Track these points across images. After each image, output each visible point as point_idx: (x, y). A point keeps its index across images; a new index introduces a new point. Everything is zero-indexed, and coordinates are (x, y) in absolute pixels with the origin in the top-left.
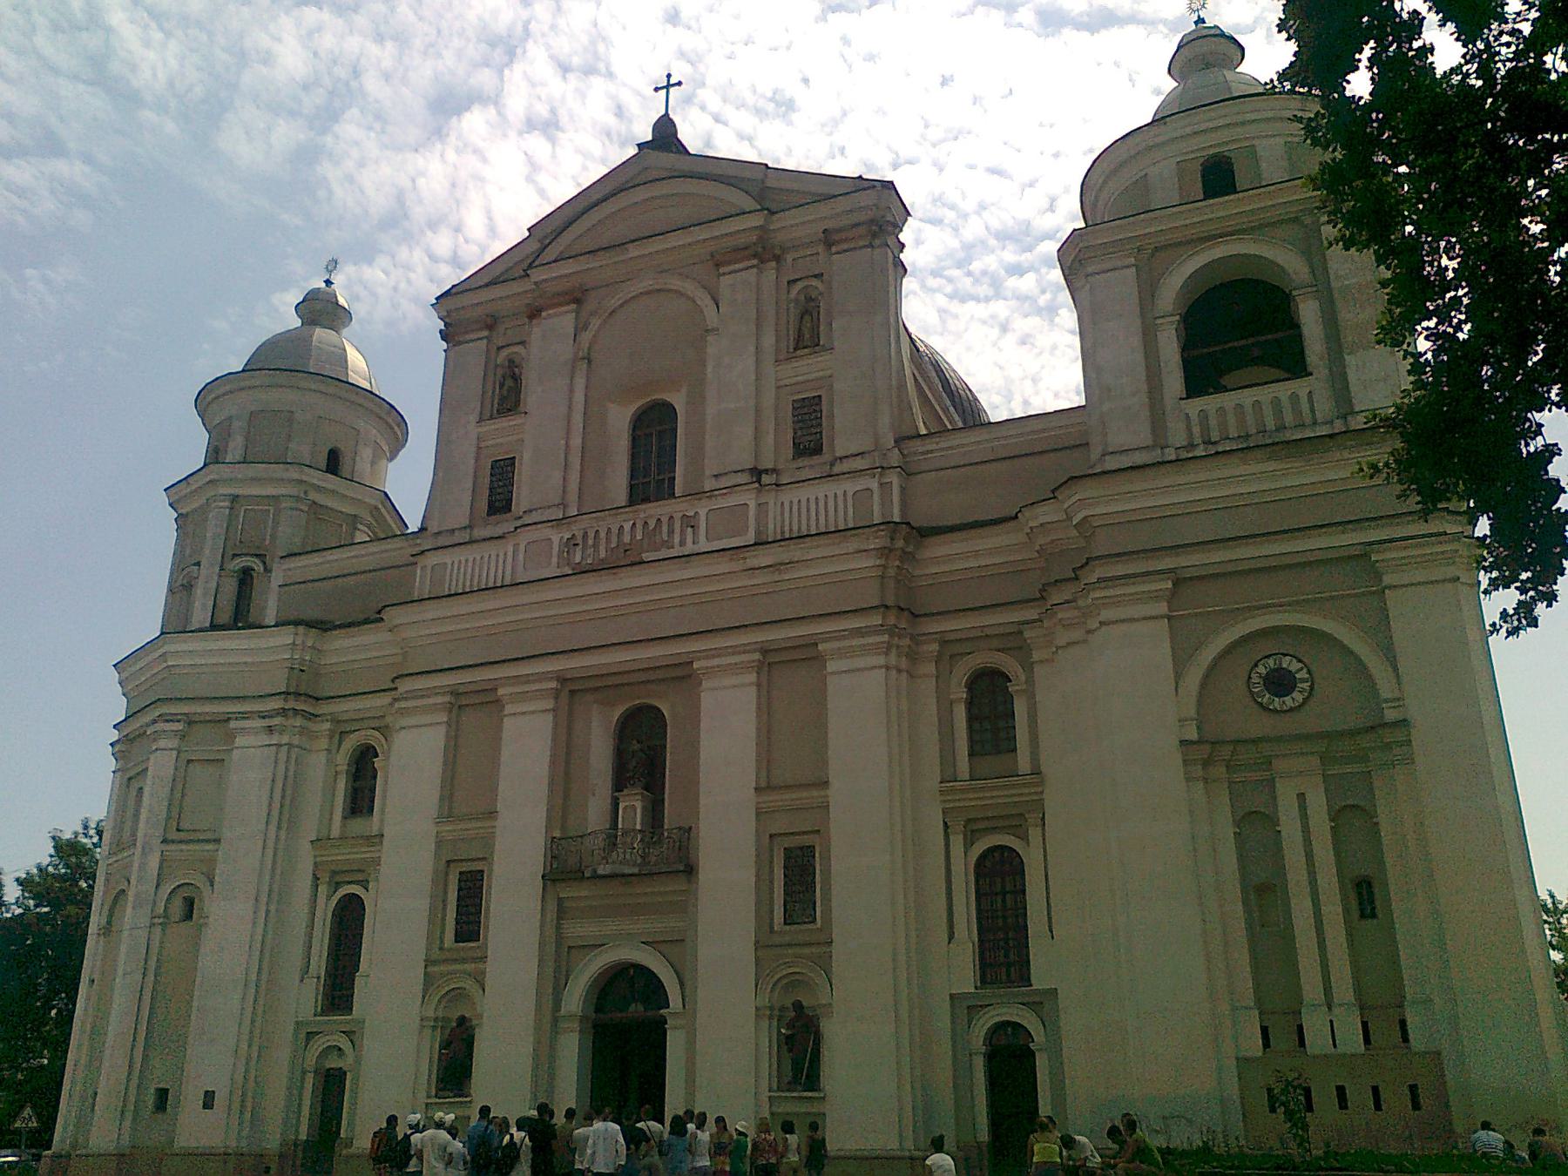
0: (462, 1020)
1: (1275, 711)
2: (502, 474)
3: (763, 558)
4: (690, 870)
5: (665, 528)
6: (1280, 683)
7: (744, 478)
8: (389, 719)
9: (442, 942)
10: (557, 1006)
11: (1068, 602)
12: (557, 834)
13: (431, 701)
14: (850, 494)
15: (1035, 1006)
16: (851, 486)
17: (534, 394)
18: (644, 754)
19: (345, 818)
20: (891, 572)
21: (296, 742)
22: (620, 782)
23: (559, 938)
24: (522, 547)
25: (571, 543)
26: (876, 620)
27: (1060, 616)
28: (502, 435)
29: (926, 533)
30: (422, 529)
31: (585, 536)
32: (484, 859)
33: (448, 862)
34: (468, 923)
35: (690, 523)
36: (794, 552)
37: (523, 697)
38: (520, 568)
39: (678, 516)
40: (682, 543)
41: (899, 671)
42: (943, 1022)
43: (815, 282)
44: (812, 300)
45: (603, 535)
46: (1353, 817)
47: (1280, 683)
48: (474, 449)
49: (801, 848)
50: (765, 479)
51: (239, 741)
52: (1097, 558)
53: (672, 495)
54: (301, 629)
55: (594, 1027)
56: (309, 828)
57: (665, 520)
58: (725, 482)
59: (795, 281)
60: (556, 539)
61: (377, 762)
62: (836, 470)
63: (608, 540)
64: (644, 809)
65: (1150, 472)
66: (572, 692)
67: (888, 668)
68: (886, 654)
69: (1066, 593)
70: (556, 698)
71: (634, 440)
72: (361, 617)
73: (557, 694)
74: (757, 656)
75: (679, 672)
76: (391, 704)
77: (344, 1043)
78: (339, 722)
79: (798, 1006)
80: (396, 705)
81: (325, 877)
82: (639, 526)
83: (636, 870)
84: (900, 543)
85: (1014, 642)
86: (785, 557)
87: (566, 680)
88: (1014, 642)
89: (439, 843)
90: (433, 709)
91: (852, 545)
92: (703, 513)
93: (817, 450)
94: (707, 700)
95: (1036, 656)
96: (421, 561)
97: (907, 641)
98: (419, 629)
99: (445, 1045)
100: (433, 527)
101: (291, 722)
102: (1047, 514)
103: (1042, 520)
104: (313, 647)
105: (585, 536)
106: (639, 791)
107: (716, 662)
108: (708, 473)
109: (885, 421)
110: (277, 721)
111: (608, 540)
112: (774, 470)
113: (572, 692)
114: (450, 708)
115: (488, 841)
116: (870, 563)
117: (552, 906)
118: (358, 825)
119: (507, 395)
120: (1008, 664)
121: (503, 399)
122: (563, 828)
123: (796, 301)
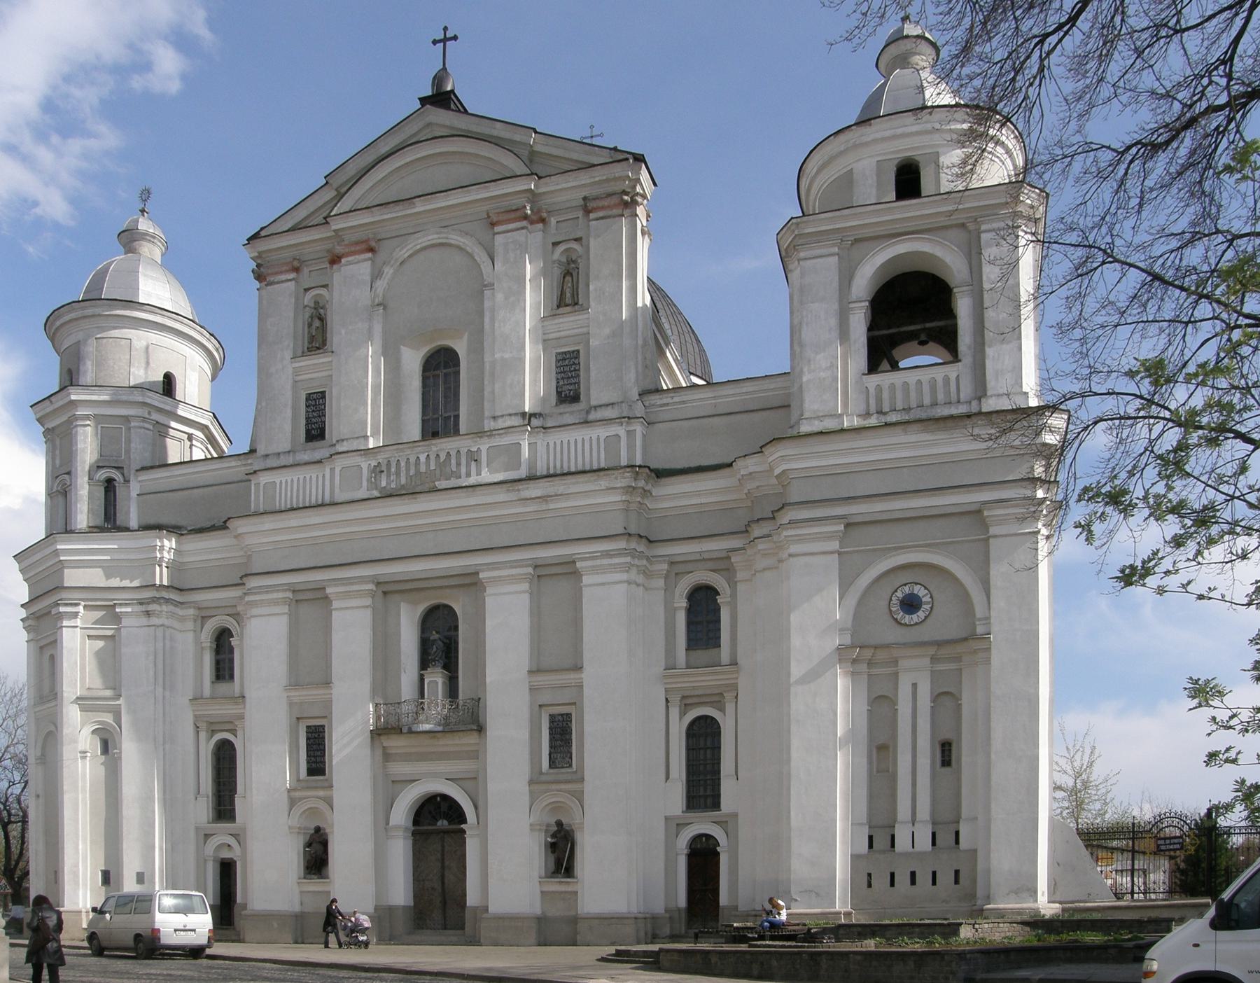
1: (906, 625)
2: (316, 404)
3: (535, 490)
5: (453, 461)
6: (911, 604)
7: (517, 421)
11: (769, 536)
13: (275, 595)
14: (602, 440)
16: (603, 432)
17: (339, 334)
18: (442, 643)
20: (634, 506)
21: (166, 622)
22: (424, 664)
25: (377, 471)
26: (621, 544)
28: (314, 369)
29: (661, 474)
30: (253, 451)
35: (474, 458)
36: (559, 486)
37: (347, 595)
38: (337, 490)
39: (464, 451)
40: (468, 475)
43: (575, 245)
44: (574, 262)
46: (946, 698)
47: (911, 604)
48: (290, 382)
50: (535, 422)
51: (125, 622)
52: (790, 504)
53: (456, 432)
57: (453, 453)
58: (501, 423)
59: (559, 243)
60: (364, 466)
62: (592, 417)
63: (408, 470)
64: (444, 683)
65: (832, 437)
66: (385, 593)
67: (629, 583)
71: (425, 379)
72: (208, 524)
73: (373, 595)
74: (530, 570)
75: (468, 580)
76: (241, 598)
80: (247, 598)
82: (433, 457)
84: (641, 483)
86: (551, 491)
87: (378, 584)
90: (275, 602)
91: (604, 483)
92: (484, 449)
93: (575, 398)
94: (490, 602)
97: (645, 562)
98: (260, 537)
100: (261, 450)
102: (751, 465)
103: (751, 469)
106: (439, 670)
108: (487, 414)
109: (631, 376)
110: (152, 607)
111: (408, 470)
112: (540, 415)
113: (385, 593)
114: (288, 602)
116: (618, 498)
119: (317, 336)
121: (312, 338)
123: (560, 262)
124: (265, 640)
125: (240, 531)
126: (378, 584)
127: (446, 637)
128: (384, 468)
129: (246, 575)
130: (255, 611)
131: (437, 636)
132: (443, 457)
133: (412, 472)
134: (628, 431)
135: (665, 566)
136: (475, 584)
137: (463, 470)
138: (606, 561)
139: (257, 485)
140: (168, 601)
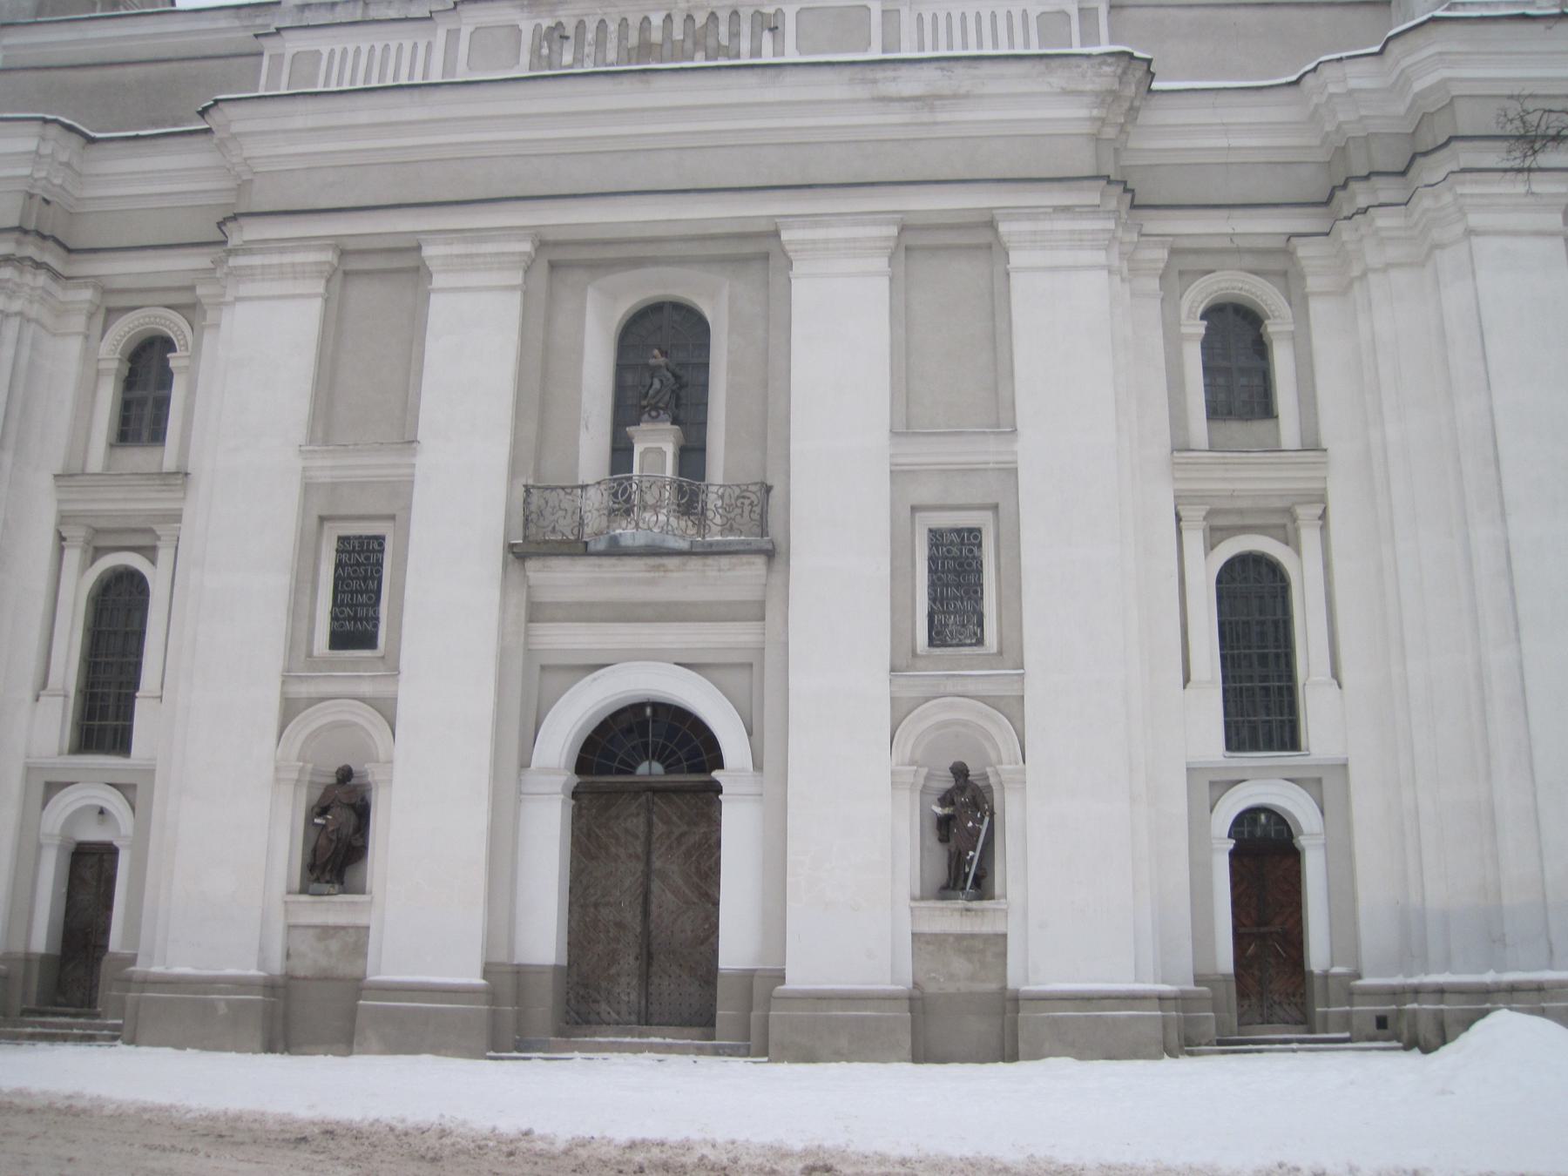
0: (345, 775)
3: (911, 83)
4: (772, 554)
5: (723, 29)
8: (200, 291)
9: (310, 642)
10: (525, 764)
12: (531, 482)
13: (299, 258)
15: (1312, 784)
19: (111, 446)
21: (34, 310)
23: (529, 652)
24: (465, 33)
25: (557, 34)
26: (1090, 196)
27: (1380, 223)
31: (581, 25)
32: (392, 518)
33: (322, 519)
34: (355, 618)
40: (756, 52)
41: (1123, 280)
42: (1178, 805)
45: (613, 27)
49: (959, 531)
54: (53, 131)
55: (575, 794)
56: (51, 453)
57: (723, 16)
60: (527, 27)
61: (175, 361)
68: (1107, 248)
69: (1387, 190)
70: (526, 272)
74: (894, 231)
75: (749, 248)
77: (115, 802)
78: (106, 292)
79: (960, 771)
80: (233, 262)
81: (77, 534)
83: (683, 545)
84: (1130, 91)
85: (1279, 261)
88: (1279, 261)
89: (308, 488)
90: (297, 272)
91: (1059, 78)
95: (1312, 283)
96: (269, 46)
98: (276, 143)
99: (323, 810)
101: (28, 278)
103: (1353, 83)
104: (68, 165)
105: (581, 25)
106: (668, 426)
107: (820, 234)
113: (553, 266)
115: (403, 490)
116: (1084, 113)
117: (518, 599)
118: (138, 458)
120: (1265, 294)
122: (537, 472)
124: (256, 362)
125: (236, 128)
126: (542, 245)
127: (681, 365)
128: (570, 31)
129: (235, 217)
130: (245, 289)
131: (661, 360)
132: (701, 19)
133: (633, 39)
134: (1081, 10)
135: (1163, 254)
136: (766, 257)
137: (745, 45)
138: (1062, 224)
139: (277, 59)
140: (38, 265)
